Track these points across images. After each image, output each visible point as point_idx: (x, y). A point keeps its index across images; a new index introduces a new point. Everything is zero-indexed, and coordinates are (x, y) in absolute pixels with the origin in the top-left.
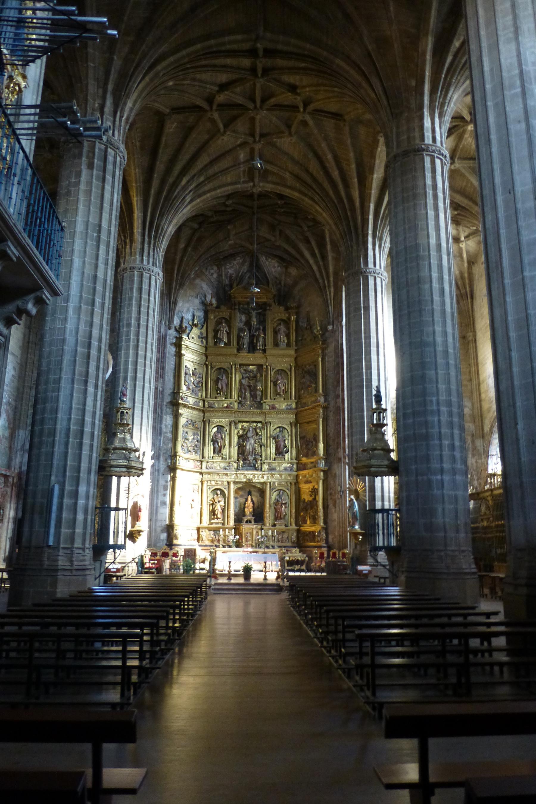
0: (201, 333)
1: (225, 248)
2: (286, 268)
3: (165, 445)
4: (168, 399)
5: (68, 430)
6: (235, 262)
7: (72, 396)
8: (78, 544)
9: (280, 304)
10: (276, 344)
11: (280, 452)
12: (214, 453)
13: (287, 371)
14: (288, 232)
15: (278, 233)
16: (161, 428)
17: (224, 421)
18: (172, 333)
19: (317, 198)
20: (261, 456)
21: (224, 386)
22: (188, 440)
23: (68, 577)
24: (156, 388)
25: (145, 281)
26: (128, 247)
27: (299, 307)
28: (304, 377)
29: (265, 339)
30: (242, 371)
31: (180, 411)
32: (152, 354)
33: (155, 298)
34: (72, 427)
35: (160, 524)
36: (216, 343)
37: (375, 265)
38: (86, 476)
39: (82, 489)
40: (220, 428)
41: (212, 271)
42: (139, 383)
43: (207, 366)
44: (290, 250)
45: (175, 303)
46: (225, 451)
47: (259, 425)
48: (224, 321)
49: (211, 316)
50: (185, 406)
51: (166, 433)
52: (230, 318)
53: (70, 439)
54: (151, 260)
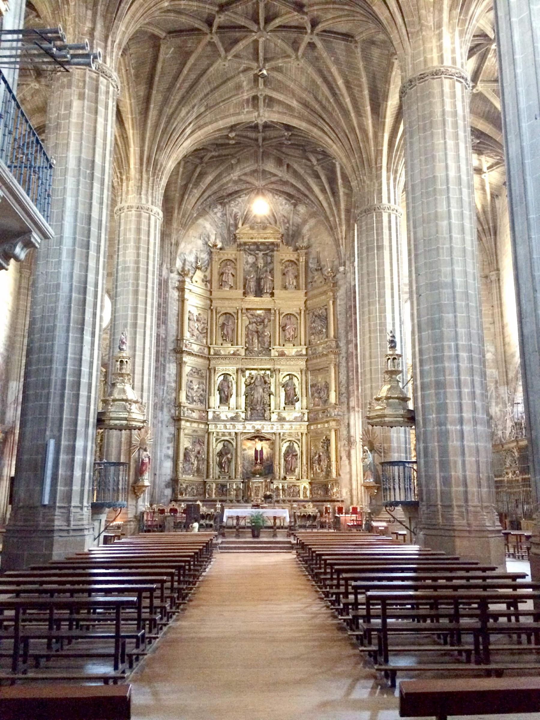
0: (205, 276)
2: (295, 205)
4: (171, 346)
5: (64, 381)
7: (67, 345)
8: (75, 502)
9: (287, 244)
10: (285, 288)
11: (291, 401)
12: (221, 402)
14: (295, 166)
15: (285, 167)
16: (164, 377)
17: (231, 369)
18: (175, 276)
19: (326, 128)
20: (270, 405)
21: (230, 332)
22: (193, 389)
23: (65, 539)
24: (158, 335)
25: (144, 221)
26: (124, 184)
27: (308, 247)
28: (314, 322)
29: (273, 281)
31: (184, 359)
32: (153, 299)
33: (155, 239)
34: (67, 378)
35: (163, 479)
37: (389, 202)
38: (83, 430)
39: (80, 444)
40: (226, 375)
41: (215, 210)
42: (140, 330)
43: (212, 310)
44: (299, 185)
45: (177, 244)
46: (232, 401)
47: (268, 372)
49: (215, 258)
50: (190, 354)
51: (169, 382)
52: (236, 260)
53: (66, 391)
54: (150, 199)
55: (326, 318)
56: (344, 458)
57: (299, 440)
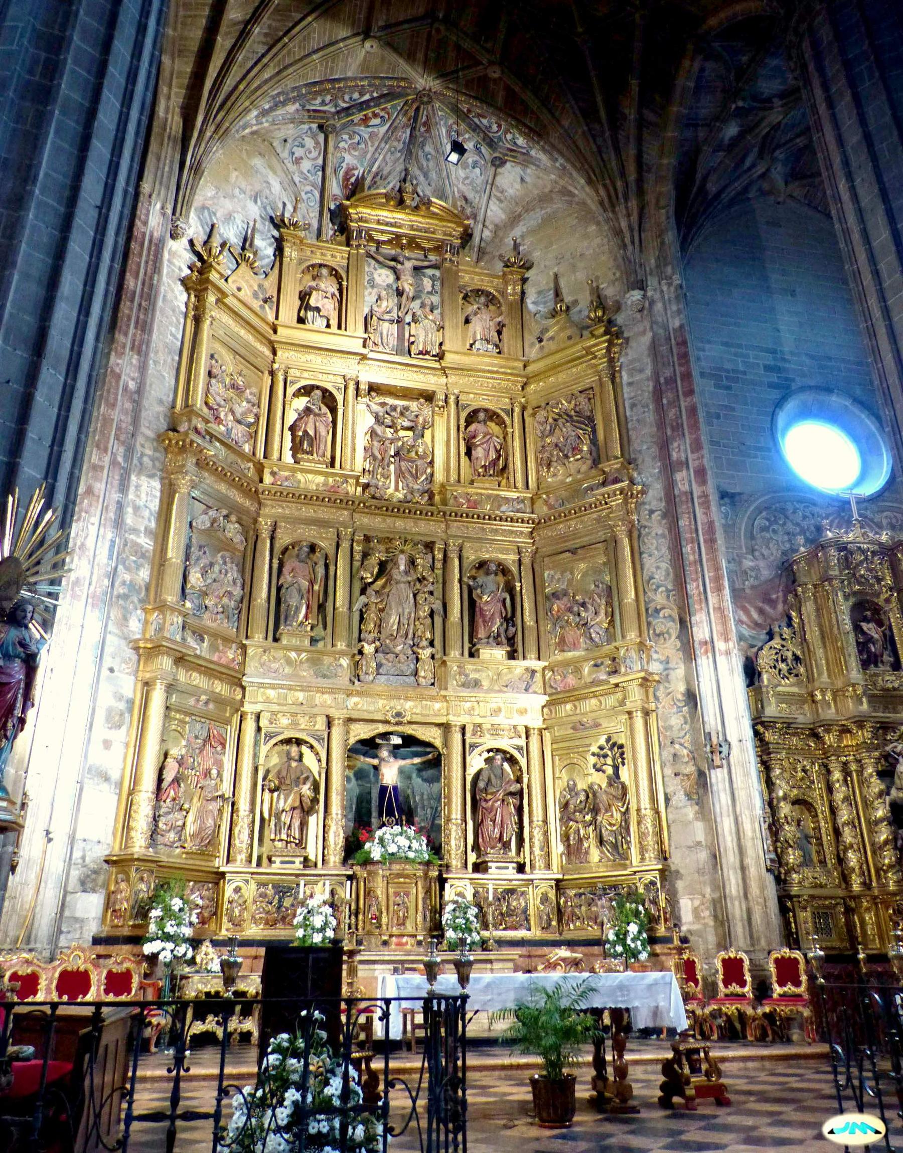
0: (260, 286)
1: (349, 74)
3: (128, 569)
6: (364, 132)
13: (503, 414)
16: (120, 506)
30: (376, 408)
36: (301, 320)
41: (299, 152)
43: (272, 373)
45: (197, 170)
48: (325, 271)
51: (135, 531)
55: (591, 419)
56: (680, 798)
57: (519, 749)
